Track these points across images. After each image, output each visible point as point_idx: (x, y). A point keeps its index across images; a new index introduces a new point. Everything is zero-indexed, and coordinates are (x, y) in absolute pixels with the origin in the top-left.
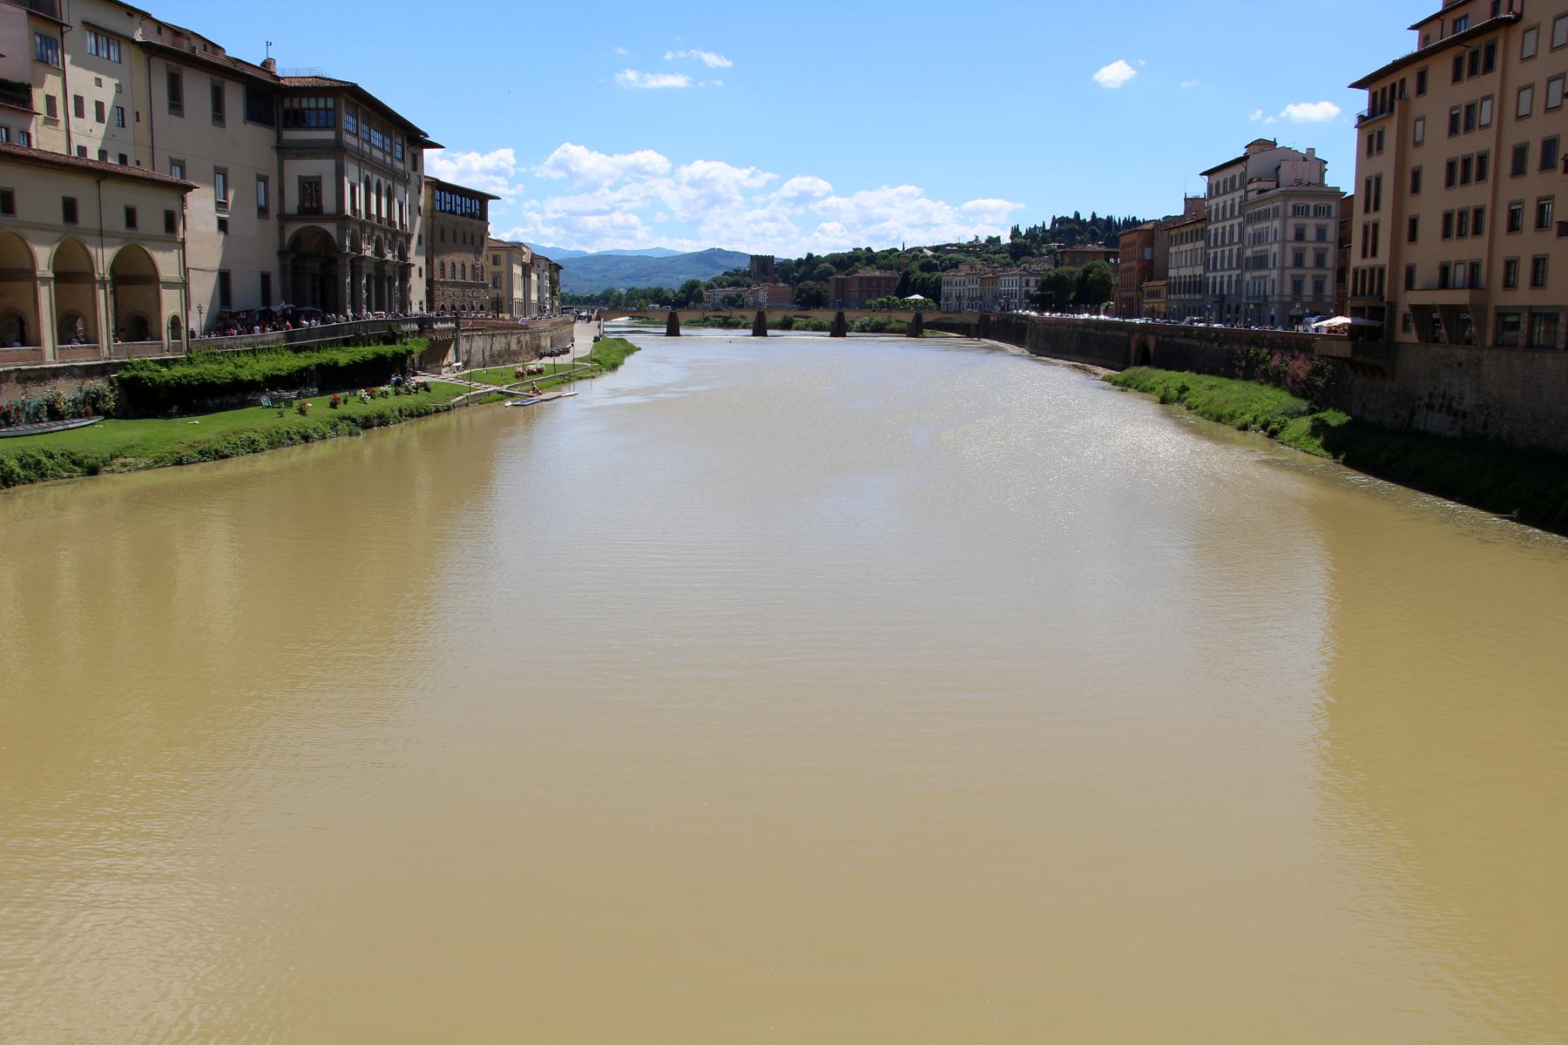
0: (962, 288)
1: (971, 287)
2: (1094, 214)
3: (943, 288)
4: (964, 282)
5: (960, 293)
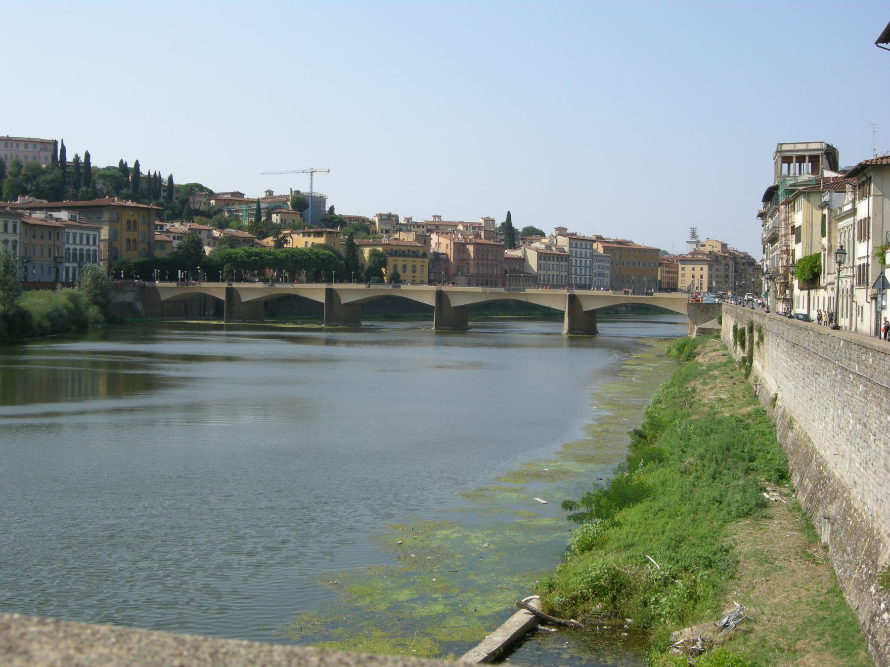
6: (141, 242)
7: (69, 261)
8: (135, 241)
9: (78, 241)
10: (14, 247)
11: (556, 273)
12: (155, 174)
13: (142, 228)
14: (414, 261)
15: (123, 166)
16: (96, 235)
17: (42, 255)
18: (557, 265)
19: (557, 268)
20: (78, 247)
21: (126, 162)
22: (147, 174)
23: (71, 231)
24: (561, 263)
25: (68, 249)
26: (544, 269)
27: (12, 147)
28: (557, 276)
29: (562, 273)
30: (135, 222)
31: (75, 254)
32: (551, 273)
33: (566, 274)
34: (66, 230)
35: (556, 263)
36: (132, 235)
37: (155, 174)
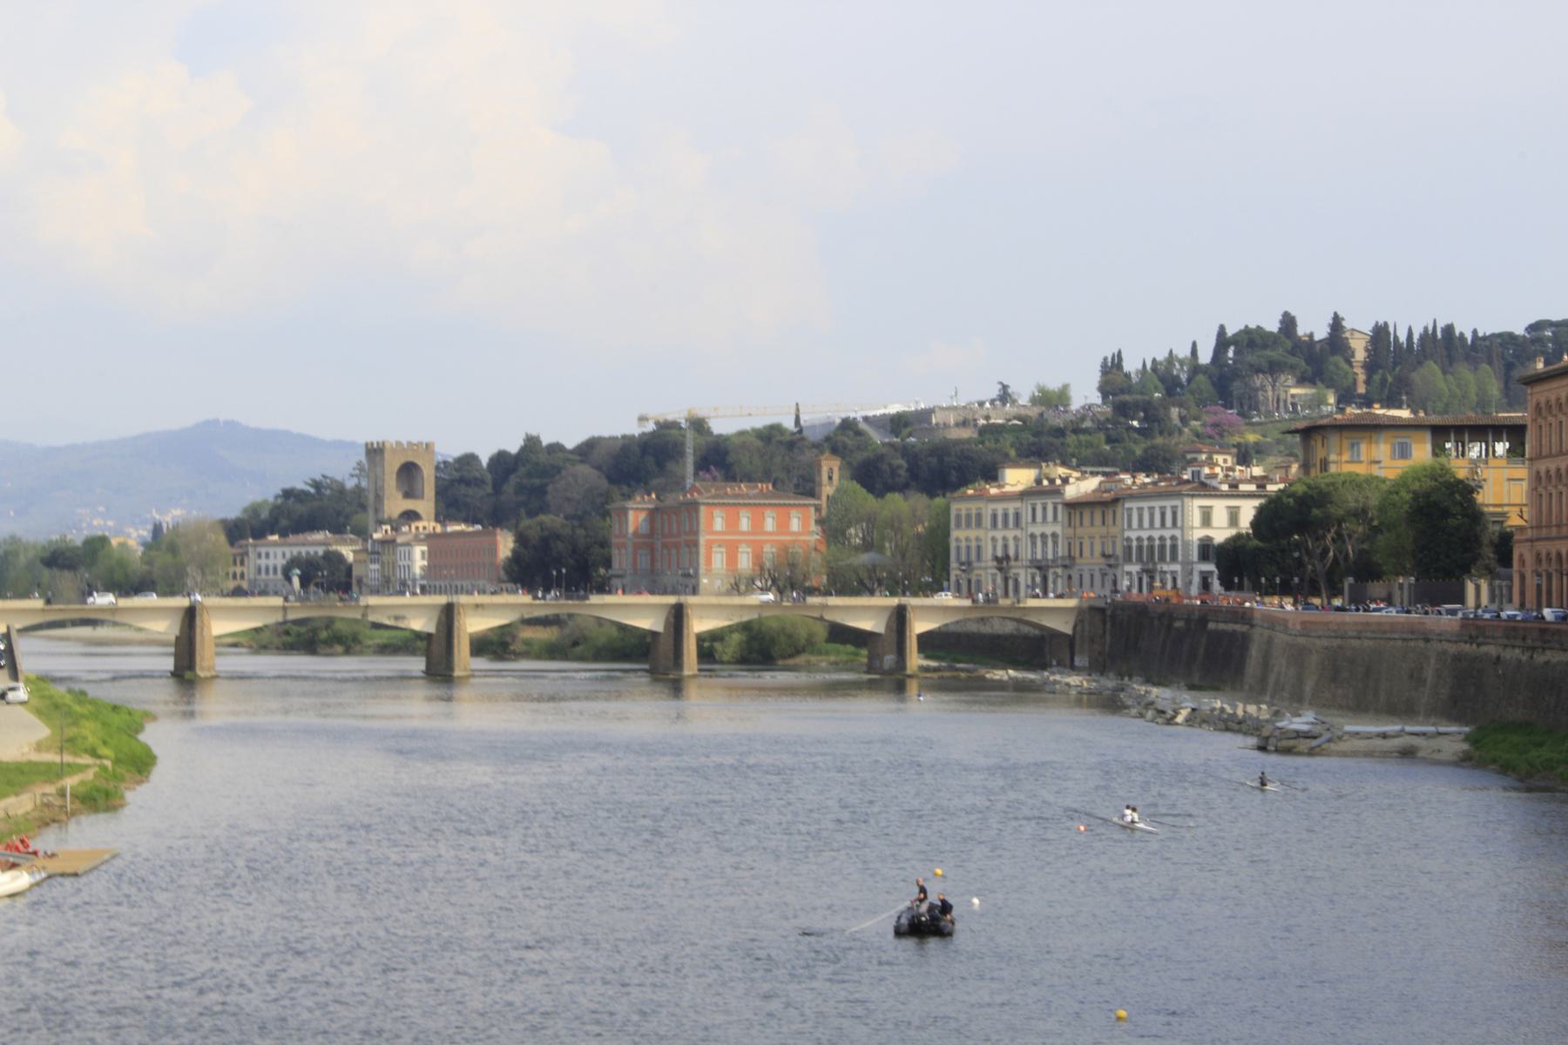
0: (1010, 534)
1: (1037, 530)
2: (1337, 323)
3: (955, 534)
4: (1017, 515)
5: (1006, 547)
7: (1128, 559)
9: (1146, 524)
10: (1055, 543)
16: (1176, 507)
17: (1092, 554)
23: (1134, 505)
25: (1129, 539)
31: (1140, 548)
34: (1127, 505)
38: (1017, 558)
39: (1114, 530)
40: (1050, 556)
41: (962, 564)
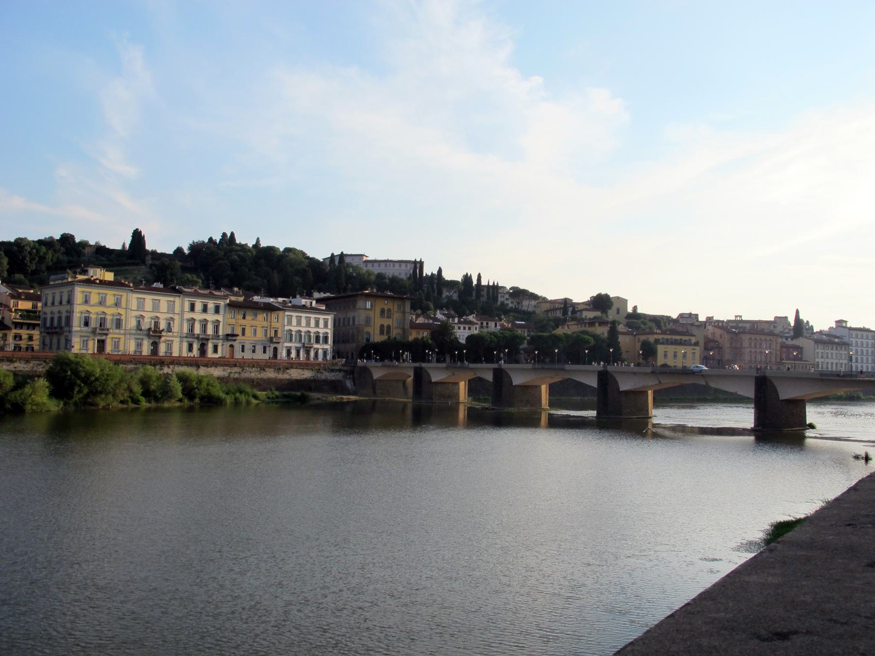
6: (395, 328)
8: (389, 327)
11: (835, 361)
12: (494, 283)
13: (397, 316)
14: (694, 349)
15: (467, 279)
18: (836, 353)
19: (836, 357)
20: (303, 330)
21: (471, 275)
22: (435, 272)
24: (841, 352)
26: (822, 357)
27: (390, 266)
28: (837, 363)
29: (841, 361)
30: (389, 310)
32: (827, 360)
33: (846, 362)
34: (287, 313)
35: (834, 352)
36: (386, 322)
37: (494, 283)
38: (169, 330)
39: (274, 325)
40: (210, 331)
41: (48, 328)
